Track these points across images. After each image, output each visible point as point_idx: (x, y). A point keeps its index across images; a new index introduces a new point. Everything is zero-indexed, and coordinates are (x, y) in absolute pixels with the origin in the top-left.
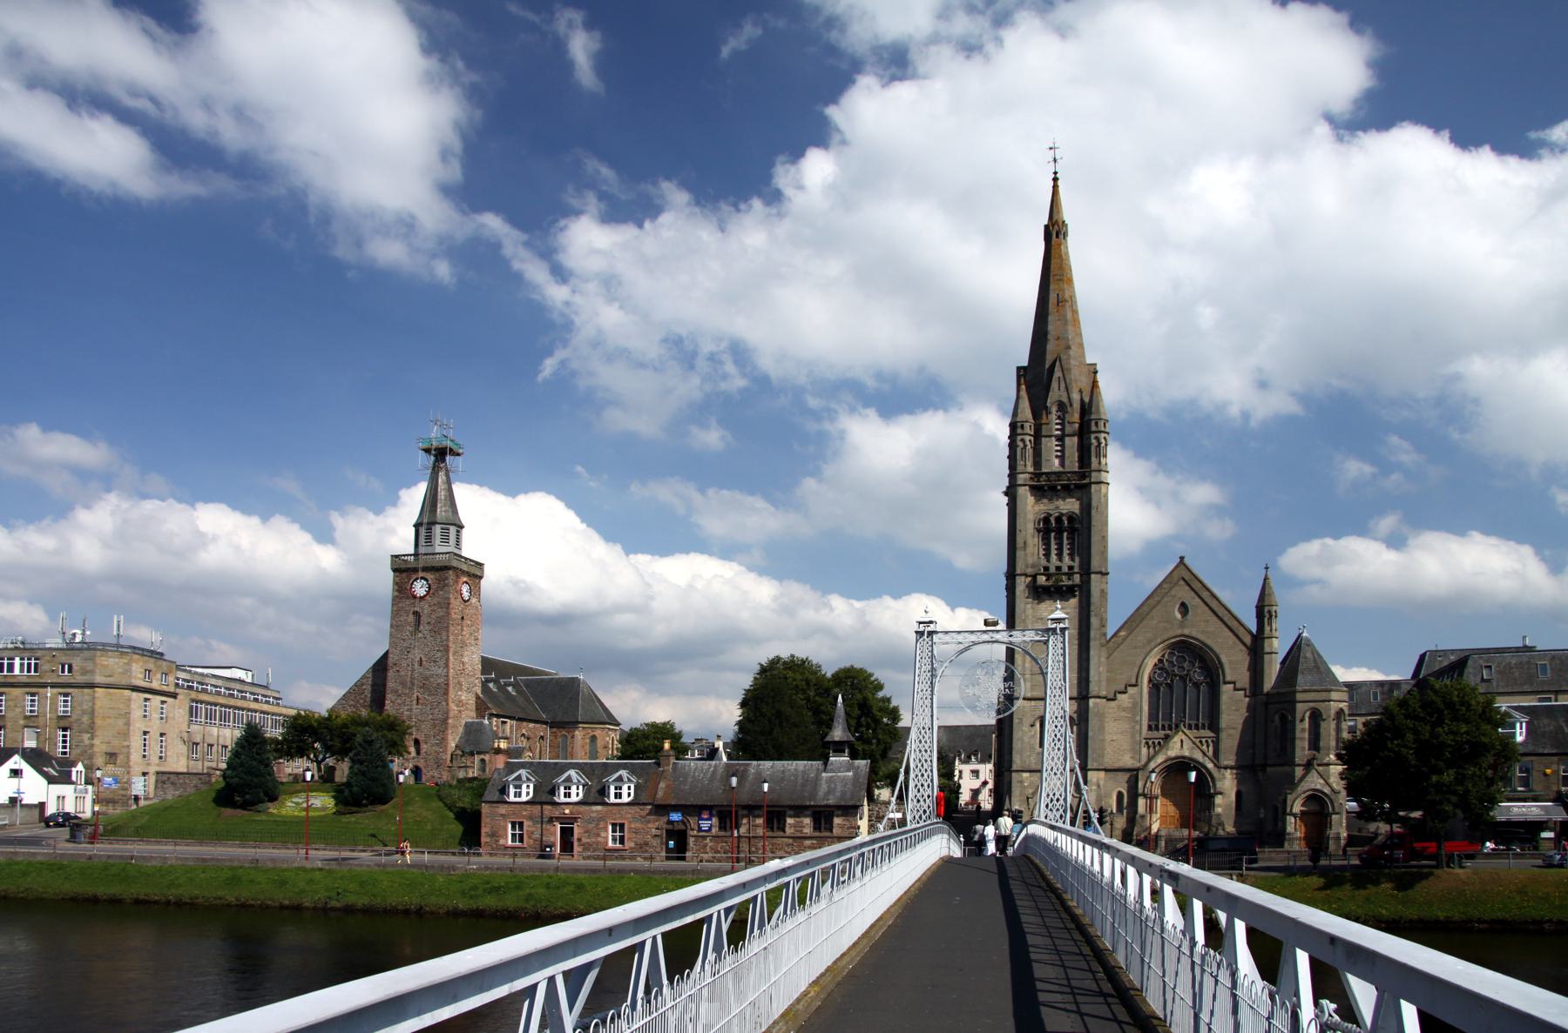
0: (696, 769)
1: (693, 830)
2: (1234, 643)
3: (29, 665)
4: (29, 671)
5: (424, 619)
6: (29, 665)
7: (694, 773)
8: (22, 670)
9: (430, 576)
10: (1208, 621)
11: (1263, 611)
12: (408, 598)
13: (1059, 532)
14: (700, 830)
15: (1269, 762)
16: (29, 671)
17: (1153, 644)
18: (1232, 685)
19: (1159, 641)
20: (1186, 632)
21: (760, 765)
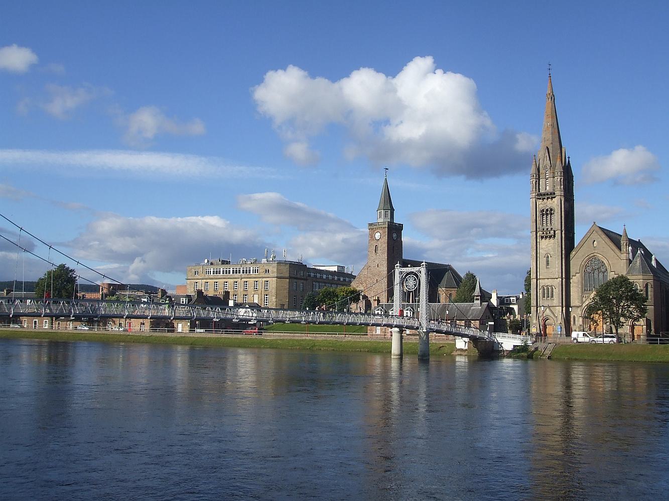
2: (614, 256)
5: (379, 248)
9: (381, 231)
10: (604, 247)
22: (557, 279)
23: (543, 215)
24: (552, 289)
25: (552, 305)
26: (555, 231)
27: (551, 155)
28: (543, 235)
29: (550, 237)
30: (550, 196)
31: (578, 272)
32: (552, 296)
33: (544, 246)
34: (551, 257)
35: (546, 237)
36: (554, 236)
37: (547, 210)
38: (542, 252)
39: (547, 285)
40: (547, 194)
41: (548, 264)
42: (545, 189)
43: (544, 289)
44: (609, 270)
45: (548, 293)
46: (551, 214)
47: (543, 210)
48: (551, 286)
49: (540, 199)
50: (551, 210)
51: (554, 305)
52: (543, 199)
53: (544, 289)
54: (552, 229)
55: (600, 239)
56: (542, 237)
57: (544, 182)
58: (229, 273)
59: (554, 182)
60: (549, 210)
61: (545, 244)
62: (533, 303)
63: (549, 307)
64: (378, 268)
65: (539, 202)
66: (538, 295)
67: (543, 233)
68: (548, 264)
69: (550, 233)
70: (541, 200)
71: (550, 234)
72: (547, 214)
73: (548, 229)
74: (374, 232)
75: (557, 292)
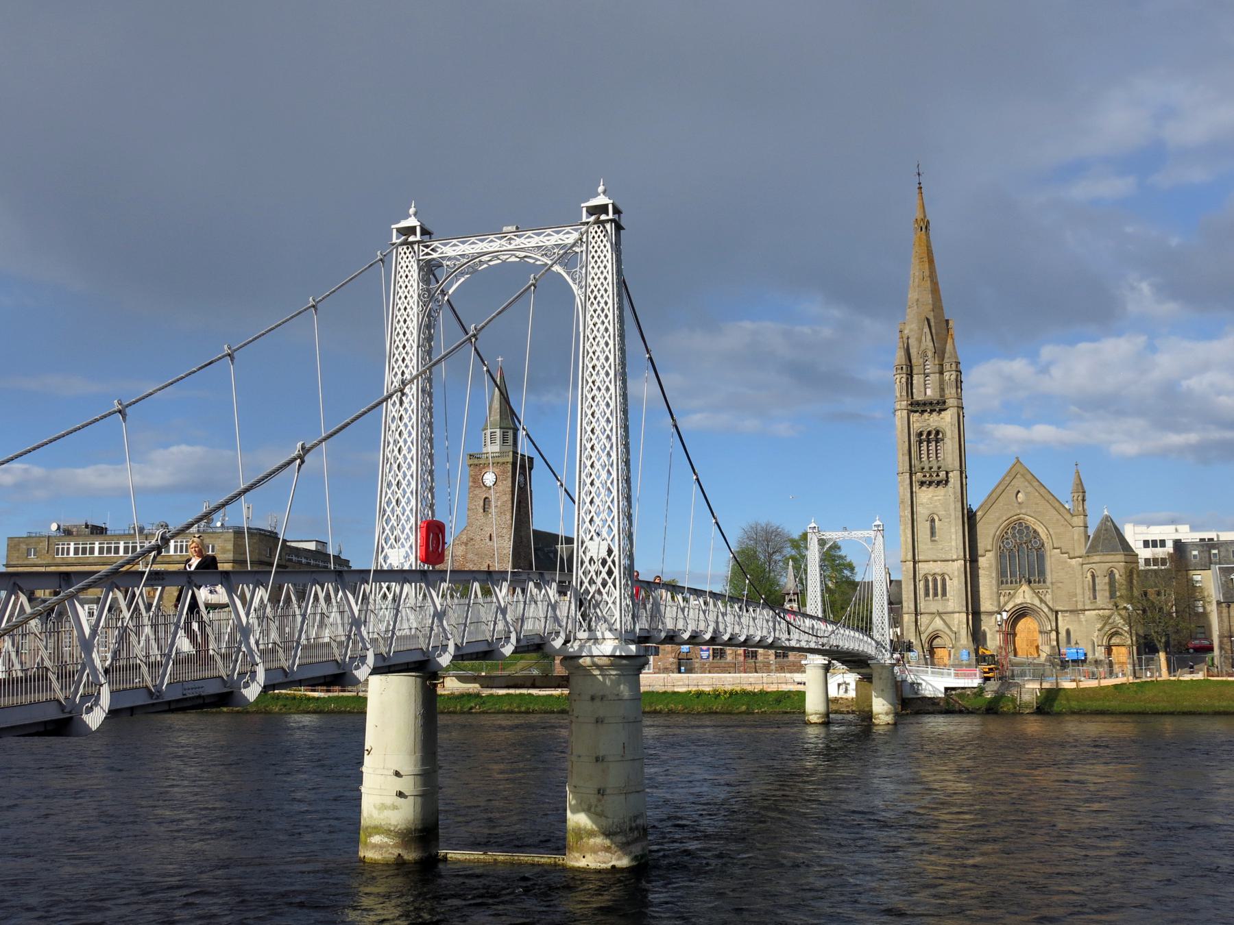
1: (697, 658)
2: (1058, 520)
3: (182, 546)
4: (181, 551)
6: (182, 546)
8: (176, 551)
9: (497, 470)
10: (1037, 504)
11: (1081, 492)
12: (480, 487)
13: (929, 442)
14: (701, 657)
15: (1087, 608)
16: (181, 551)
17: (1001, 521)
18: (1059, 550)
19: (1005, 518)
20: (1023, 511)
22: (953, 561)
23: (920, 442)
24: (944, 581)
25: (945, 611)
26: (947, 473)
27: (933, 331)
28: (924, 479)
29: (938, 483)
30: (920, 409)
31: (989, 548)
32: (944, 593)
33: (925, 501)
34: (940, 520)
35: (930, 484)
36: (947, 482)
37: (929, 433)
38: (922, 512)
39: (933, 572)
40: (931, 403)
41: (933, 533)
42: (923, 393)
43: (927, 581)
44: (1048, 546)
45: (937, 587)
46: (937, 441)
47: (921, 434)
48: (943, 575)
50: (937, 433)
51: (950, 609)
52: (923, 412)
53: (927, 581)
54: (939, 468)
55: (1030, 489)
56: (922, 484)
57: (922, 380)
58: (68, 553)
59: (942, 382)
60: (934, 432)
61: (925, 496)
62: (909, 607)
63: (939, 614)
64: (490, 543)
65: (915, 417)
67: (925, 476)
68: (933, 533)
69: (938, 475)
70: (917, 414)
71: (938, 479)
72: (929, 442)
73: (931, 468)
74: (480, 470)
75: (956, 586)
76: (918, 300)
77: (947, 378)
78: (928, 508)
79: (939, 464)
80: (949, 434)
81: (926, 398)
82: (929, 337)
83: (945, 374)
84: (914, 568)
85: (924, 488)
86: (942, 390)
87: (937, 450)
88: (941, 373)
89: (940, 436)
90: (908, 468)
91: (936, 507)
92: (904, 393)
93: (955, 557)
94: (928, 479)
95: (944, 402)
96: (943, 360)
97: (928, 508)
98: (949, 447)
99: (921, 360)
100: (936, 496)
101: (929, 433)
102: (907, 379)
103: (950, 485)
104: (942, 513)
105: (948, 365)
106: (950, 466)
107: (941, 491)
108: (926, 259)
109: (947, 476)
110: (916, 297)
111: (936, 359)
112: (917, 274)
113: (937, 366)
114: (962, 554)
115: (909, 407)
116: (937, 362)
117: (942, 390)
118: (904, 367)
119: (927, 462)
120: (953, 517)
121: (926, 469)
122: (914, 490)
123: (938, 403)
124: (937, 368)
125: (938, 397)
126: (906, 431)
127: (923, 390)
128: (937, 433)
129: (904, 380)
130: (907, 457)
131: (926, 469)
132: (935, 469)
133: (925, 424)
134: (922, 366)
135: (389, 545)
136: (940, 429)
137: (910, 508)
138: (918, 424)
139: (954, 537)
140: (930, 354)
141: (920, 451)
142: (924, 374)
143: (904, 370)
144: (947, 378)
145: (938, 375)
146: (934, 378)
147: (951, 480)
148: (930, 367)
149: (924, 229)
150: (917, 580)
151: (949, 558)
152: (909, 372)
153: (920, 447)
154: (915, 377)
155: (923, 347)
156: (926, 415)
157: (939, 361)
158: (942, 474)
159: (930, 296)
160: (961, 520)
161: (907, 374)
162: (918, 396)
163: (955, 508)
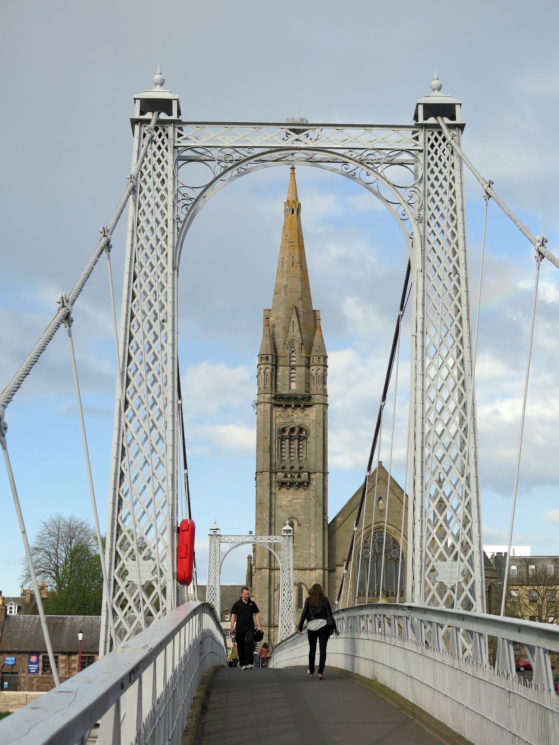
0: (24, 621)
1: (24, 672)
7: (23, 625)
14: (29, 671)
21: (73, 619)
22: (311, 570)
23: (282, 439)
26: (309, 474)
27: (301, 321)
28: (285, 480)
29: (301, 485)
30: (284, 403)
33: (284, 503)
34: (299, 525)
35: (292, 484)
36: (309, 483)
37: (292, 430)
40: (296, 398)
42: (288, 387)
46: (300, 439)
47: (283, 430)
49: (281, 406)
52: (288, 406)
54: (301, 468)
56: (282, 484)
57: (287, 373)
59: (308, 376)
60: (297, 430)
65: (278, 411)
66: (272, 602)
67: (286, 476)
69: (299, 476)
70: (280, 409)
71: (300, 480)
72: (291, 439)
73: (292, 468)
76: (286, 287)
77: (314, 372)
78: (287, 512)
79: (301, 464)
80: (312, 432)
81: (291, 392)
82: (297, 327)
83: (312, 368)
84: (270, 576)
85: (284, 490)
86: (308, 384)
87: (299, 449)
88: (308, 366)
89: (304, 433)
90: (269, 466)
91: (295, 510)
92: (268, 385)
93: (313, 566)
94: (289, 479)
95: (310, 398)
96: (310, 353)
97: (287, 512)
98: (312, 444)
99: (288, 352)
100: (297, 499)
101: (292, 430)
102: (273, 369)
103: (312, 487)
104: (302, 517)
105: (316, 359)
106: (312, 467)
107: (301, 494)
108: (296, 244)
109: (309, 478)
110: (285, 283)
111: (303, 350)
112: (286, 259)
113: (304, 359)
114: (321, 563)
115: (273, 401)
116: (303, 355)
117: (308, 384)
118: (270, 357)
119: (288, 461)
120: (313, 522)
121: (288, 469)
122: (273, 491)
123: (303, 398)
124: (303, 361)
125: (302, 392)
126: (268, 426)
127: (287, 383)
128: (301, 430)
129: (268, 371)
130: (268, 455)
131: (288, 469)
132: (296, 469)
133: (288, 420)
134: (288, 358)
135: (436, 556)
136: (304, 427)
137: (268, 511)
138: (281, 420)
139: (313, 544)
140: (297, 346)
141: (282, 448)
142: (290, 366)
143: (270, 361)
144: (314, 372)
145: (304, 368)
146: (301, 371)
147: (313, 483)
148: (297, 359)
149: (295, 213)
150: (272, 590)
151: (307, 566)
152: (274, 363)
153: (282, 444)
154: (280, 369)
155: (290, 337)
156: (290, 411)
157: (305, 353)
158: (304, 476)
159: (299, 283)
160: (322, 526)
161: (273, 365)
162: (283, 390)
163: (316, 512)
